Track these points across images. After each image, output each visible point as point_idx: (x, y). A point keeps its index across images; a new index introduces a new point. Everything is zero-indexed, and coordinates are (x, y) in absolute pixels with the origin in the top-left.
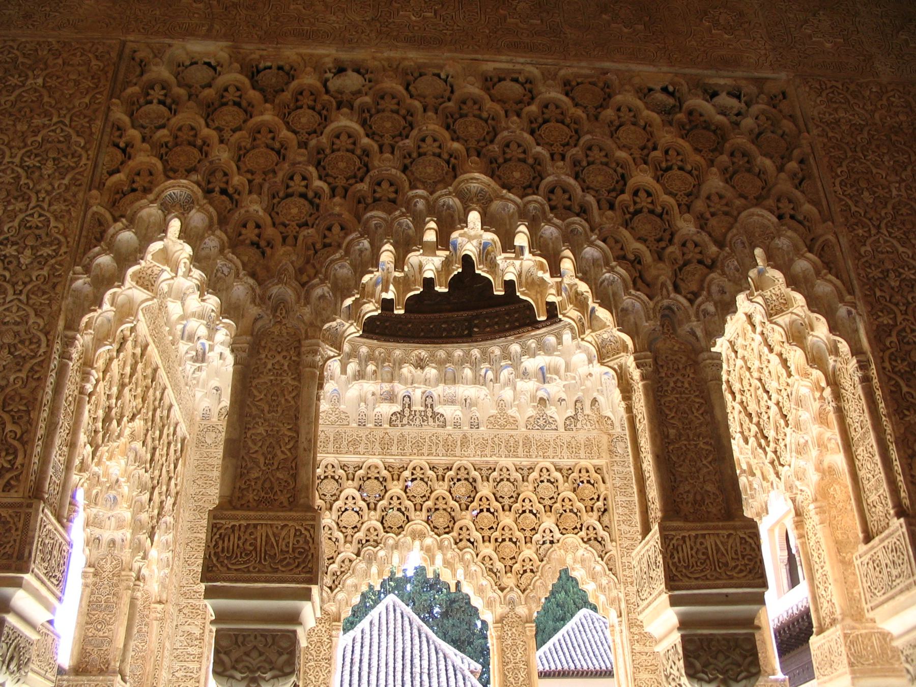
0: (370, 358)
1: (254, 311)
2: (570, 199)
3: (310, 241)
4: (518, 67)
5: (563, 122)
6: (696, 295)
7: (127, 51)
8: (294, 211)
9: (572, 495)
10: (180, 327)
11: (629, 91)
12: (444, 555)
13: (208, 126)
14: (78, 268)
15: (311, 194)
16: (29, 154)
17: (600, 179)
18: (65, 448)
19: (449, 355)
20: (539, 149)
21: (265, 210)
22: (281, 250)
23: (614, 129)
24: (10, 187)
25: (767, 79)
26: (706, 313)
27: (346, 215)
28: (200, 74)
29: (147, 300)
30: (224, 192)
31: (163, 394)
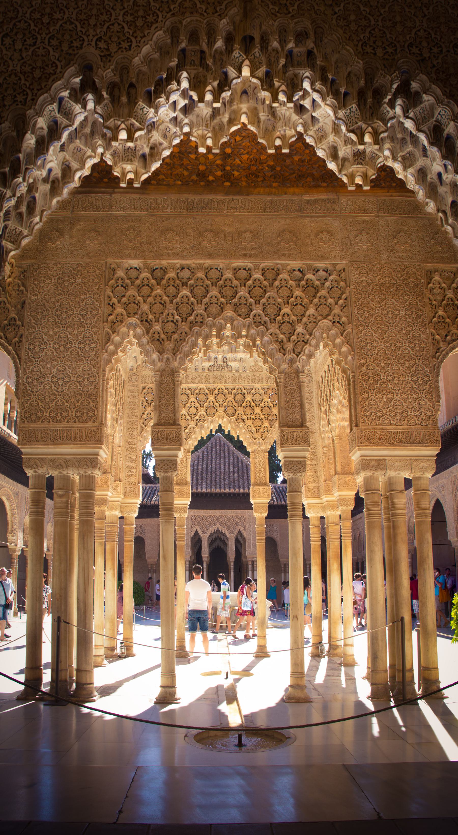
1: (159, 364)
4: (246, 264)
5: (260, 287)
6: (300, 353)
7: (108, 265)
8: (170, 328)
14: (104, 351)
15: (175, 321)
17: (272, 310)
20: (251, 300)
22: (167, 343)
23: (279, 288)
26: (303, 359)
27: (187, 329)
28: (133, 273)
30: (146, 321)
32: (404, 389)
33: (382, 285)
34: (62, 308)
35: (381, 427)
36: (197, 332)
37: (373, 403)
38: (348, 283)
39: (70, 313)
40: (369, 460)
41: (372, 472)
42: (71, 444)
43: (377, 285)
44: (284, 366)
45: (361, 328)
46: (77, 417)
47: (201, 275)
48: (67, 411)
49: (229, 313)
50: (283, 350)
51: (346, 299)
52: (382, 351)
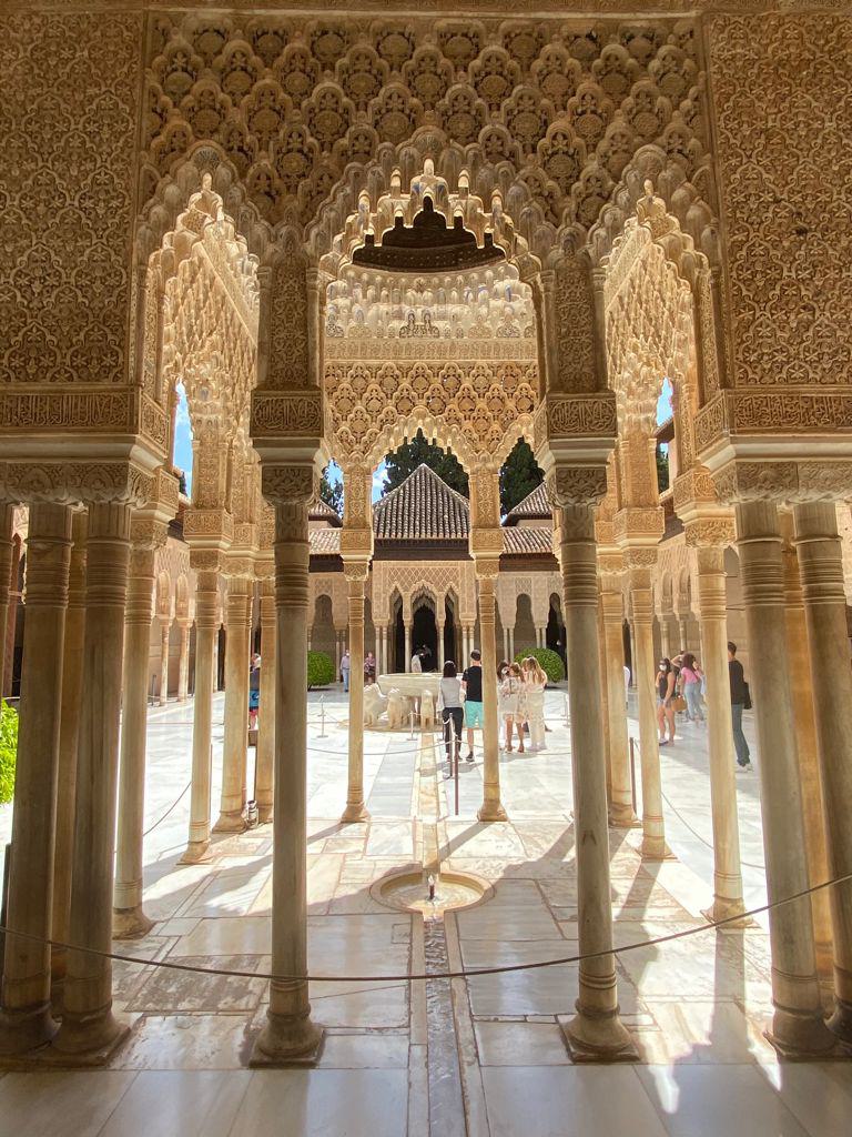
0: (383, 285)
1: (270, 248)
2: (502, 145)
3: (307, 189)
4: (467, 22)
5: (501, 74)
7: (150, 19)
8: (294, 164)
9: (527, 385)
10: (239, 263)
11: (558, 40)
12: (439, 429)
13: (223, 91)
14: (141, 217)
15: (306, 150)
16: (88, 121)
17: (527, 125)
18: (153, 352)
19: (441, 281)
20: (479, 101)
21: (271, 165)
23: (543, 76)
24: (79, 151)
25: (677, 19)
27: (332, 167)
28: (212, 41)
29: (196, 241)
30: (241, 149)
31: (232, 316)
32: (839, 297)
33: (781, 64)
34: (43, 117)
35: (785, 387)
36: (357, 175)
37: (764, 331)
38: (701, 62)
39: (61, 127)
40: (756, 465)
41: (764, 493)
42: (59, 431)
43: (768, 65)
44: (557, 253)
45: (733, 161)
46: (77, 368)
47: (365, 45)
48: (52, 354)
49: (429, 132)
50: (554, 215)
51: (696, 99)
52: (784, 213)
